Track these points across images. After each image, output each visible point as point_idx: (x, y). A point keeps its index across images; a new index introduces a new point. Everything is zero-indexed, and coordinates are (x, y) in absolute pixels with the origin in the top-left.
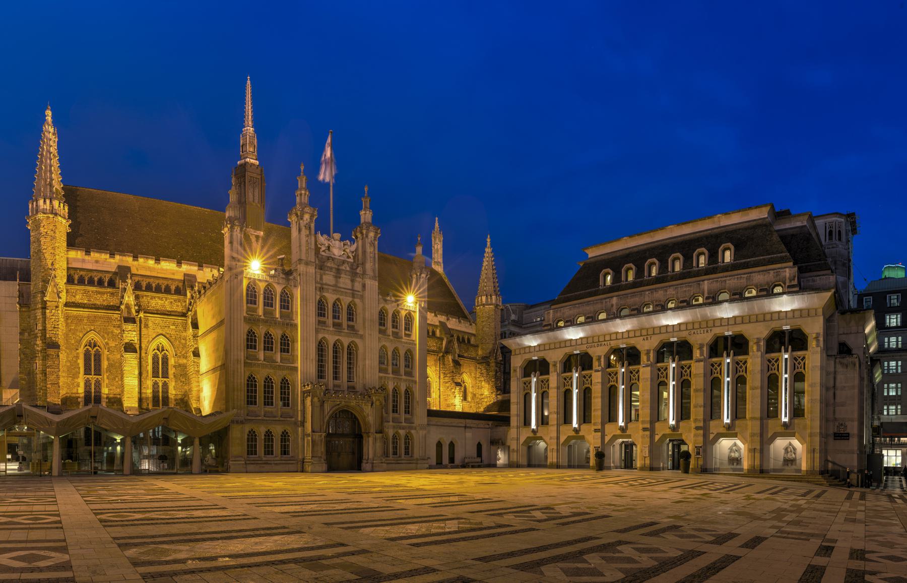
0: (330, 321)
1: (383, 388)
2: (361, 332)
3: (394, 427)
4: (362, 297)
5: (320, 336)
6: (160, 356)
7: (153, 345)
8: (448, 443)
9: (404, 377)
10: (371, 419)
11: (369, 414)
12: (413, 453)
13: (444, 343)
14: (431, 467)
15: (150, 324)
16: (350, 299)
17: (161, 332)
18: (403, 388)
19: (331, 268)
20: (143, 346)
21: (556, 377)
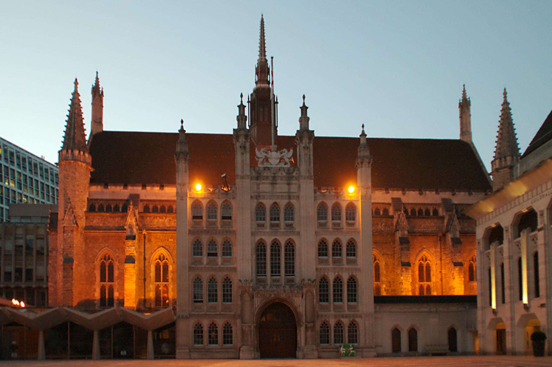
0: (268, 222)
2: (297, 230)
3: (335, 316)
4: (298, 197)
5: (257, 238)
6: (162, 264)
7: (156, 256)
9: (346, 266)
10: (301, 309)
11: (300, 304)
12: (359, 342)
15: (153, 239)
16: (287, 201)
17: (161, 244)
18: (345, 277)
19: (267, 178)
20: (147, 257)
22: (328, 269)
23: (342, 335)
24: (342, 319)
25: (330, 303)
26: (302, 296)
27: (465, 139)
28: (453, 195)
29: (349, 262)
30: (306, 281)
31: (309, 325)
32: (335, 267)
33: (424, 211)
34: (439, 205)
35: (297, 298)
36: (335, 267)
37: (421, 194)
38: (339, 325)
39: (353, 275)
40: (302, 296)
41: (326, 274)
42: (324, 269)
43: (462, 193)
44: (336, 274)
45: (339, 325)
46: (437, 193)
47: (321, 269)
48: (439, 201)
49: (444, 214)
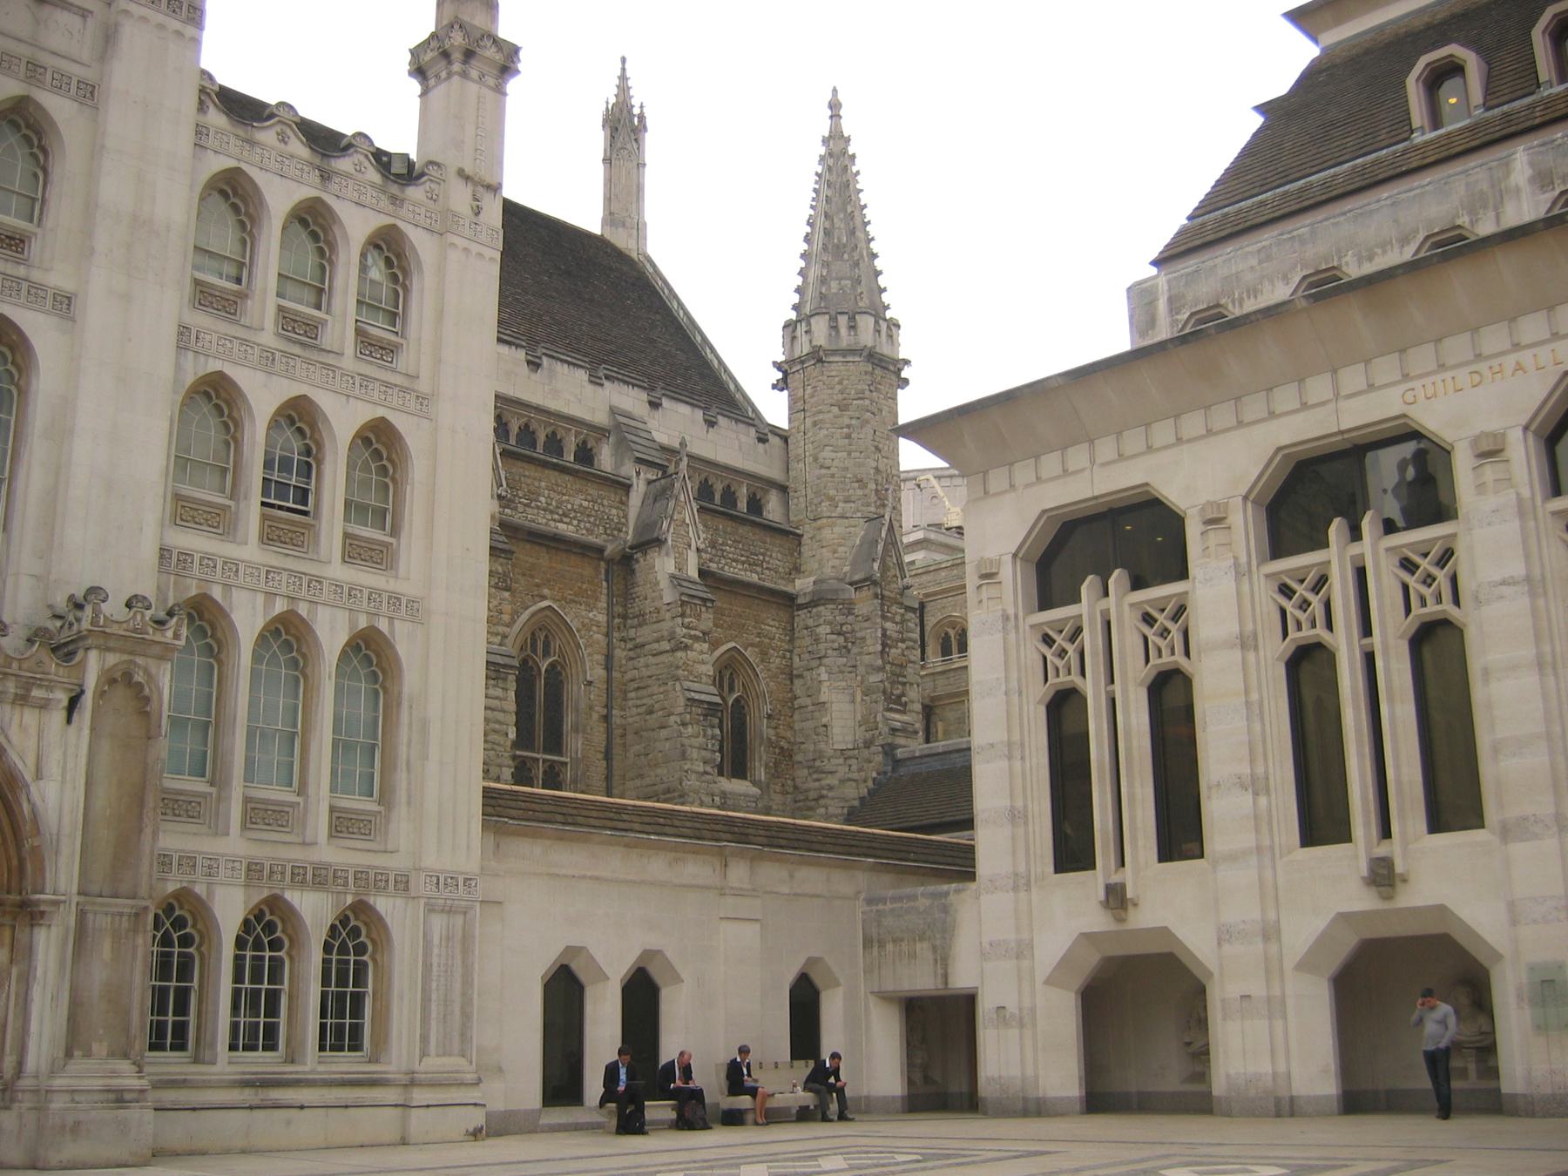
1: (204, 617)
8: (617, 969)
9: (338, 571)
12: (382, 1040)
13: (635, 499)
14: (498, 1126)
18: (331, 632)
21: (1227, 585)
22: (232, 565)
23: (273, 997)
24: (293, 897)
25: (219, 780)
26: (73, 704)
27: (621, 240)
28: (655, 405)
29: (354, 550)
30: (113, 608)
31: (99, 922)
32: (276, 561)
33: (541, 438)
34: (602, 432)
35: (30, 717)
36: (276, 561)
37: (534, 365)
38: (267, 929)
39: (372, 629)
40: (73, 704)
41: (217, 593)
42: (208, 560)
43: (684, 409)
44: (280, 606)
45: (267, 929)
46: (595, 381)
47: (185, 558)
48: (601, 418)
49: (628, 469)
